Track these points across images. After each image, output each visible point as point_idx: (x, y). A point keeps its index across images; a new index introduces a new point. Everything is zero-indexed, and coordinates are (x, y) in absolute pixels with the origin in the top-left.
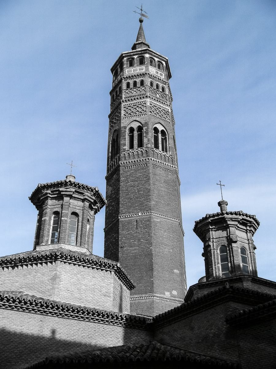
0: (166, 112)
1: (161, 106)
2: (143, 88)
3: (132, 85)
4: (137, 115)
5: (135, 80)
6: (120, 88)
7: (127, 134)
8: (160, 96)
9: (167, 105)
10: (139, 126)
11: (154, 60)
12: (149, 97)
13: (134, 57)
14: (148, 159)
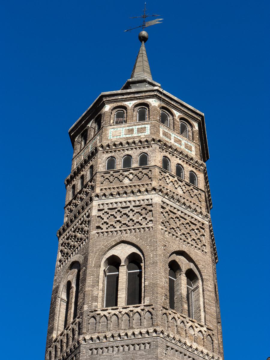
0: (198, 229)
1: (186, 214)
2: (145, 171)
3: (119, 165)
4: (130, 230)
5: (127, 152)
6: (92, 167)
7: (102, 274)
8: (184, 193)
9: (201, 213)
10: (133, 255)
12: (160, 190)
13: (127, 103)
14: (155, 331)
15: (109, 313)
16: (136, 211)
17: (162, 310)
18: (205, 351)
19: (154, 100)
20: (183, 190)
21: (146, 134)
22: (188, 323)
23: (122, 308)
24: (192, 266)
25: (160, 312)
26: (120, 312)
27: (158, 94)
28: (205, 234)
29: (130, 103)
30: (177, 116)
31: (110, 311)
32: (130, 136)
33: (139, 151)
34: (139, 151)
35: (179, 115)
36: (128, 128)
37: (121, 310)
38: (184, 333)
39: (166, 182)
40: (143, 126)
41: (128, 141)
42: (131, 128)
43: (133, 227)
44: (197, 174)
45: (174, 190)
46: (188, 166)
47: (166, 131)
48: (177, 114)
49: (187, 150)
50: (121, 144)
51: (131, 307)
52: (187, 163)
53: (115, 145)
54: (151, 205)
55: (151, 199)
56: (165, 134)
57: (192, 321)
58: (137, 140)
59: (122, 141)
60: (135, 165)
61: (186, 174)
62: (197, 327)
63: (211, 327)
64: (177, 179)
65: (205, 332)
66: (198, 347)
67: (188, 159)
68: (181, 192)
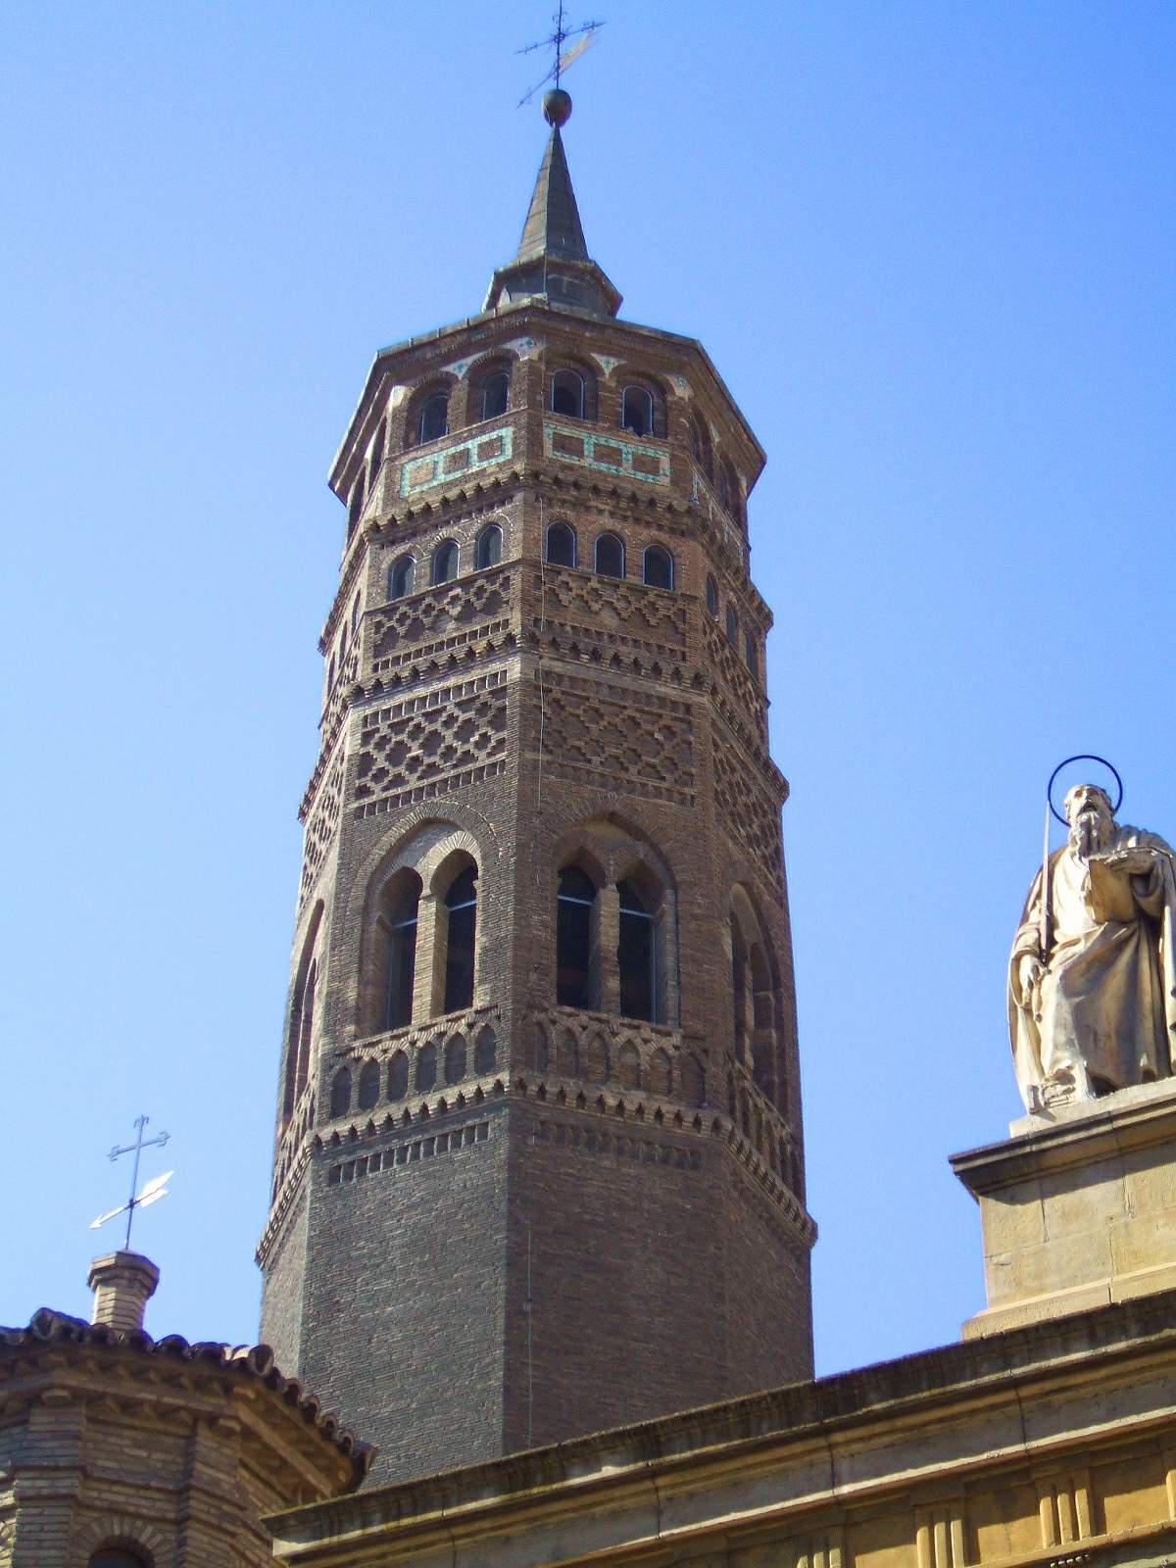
1: (624, 691)
5: (444, 533)
11: (594, 370)
13: (451, 368)
15: (385, 1051)
16: (462, 717)
17: (525, 1017)
18: (668, 1109)
19: (525, 340)
20: (619, 614)
21: (501, 460)
22: (615, 1034)
23: (421, 1029)
24: (642, 850)
25: (520, 1022)
26: (413, 1043)
27: (534, 320)
28: (692, 739)
29: (461, 367)
30: (607, 372)
31: (387, 1044)
32: (458, 474)
33: (476, 524)
34: (476, 524)
35: (616, 364)
36: (452, 450)
37: (416, 1035)
38: (601, 1068)
39: (560, 601)
40: (494, 435)
41: (448, 495)
42: (461, 447)
43: (453, 773)
44: (672, 545)
45: (587, 623)
46: (638, 529)
47: (566, 432)
48: (607, 364)
49: (640, 476)
50: (428, 508)
51: (442, 1024)
52: (637, 521)
53: (410, 515)
54: (504, 689)
55: (505, 671)
56: (562, 444)
57: (630, 1027)
58: (469, 488)
59: (430, 499)
60: (464, 571)
61: (634, 556)
62: (646, 1041)
63: (698, 1026)
64: (599, 582)
65: (677, 1048)
66: (645, 1103)
67: (639, 506)
68: (614, 621)
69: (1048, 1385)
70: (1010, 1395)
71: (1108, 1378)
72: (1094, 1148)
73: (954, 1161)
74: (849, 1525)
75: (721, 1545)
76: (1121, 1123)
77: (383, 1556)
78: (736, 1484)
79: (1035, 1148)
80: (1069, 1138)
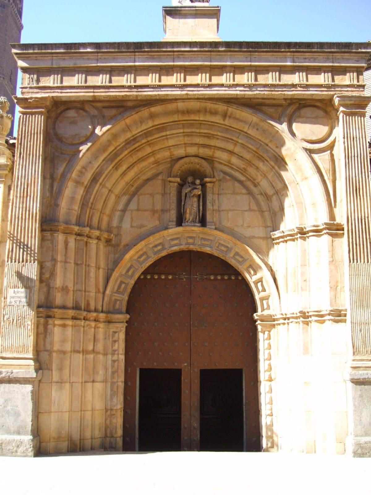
69: (180, 53)
70: (172, 54)
71: (191, 55)
72: (191, 12)
73: (163, 7)
74: (136, 70)
75: (109, 69)
76: (197, 8)
77: (36, 57)
78: (114, 58)
79: (180, 9)
80: (187, 9)
